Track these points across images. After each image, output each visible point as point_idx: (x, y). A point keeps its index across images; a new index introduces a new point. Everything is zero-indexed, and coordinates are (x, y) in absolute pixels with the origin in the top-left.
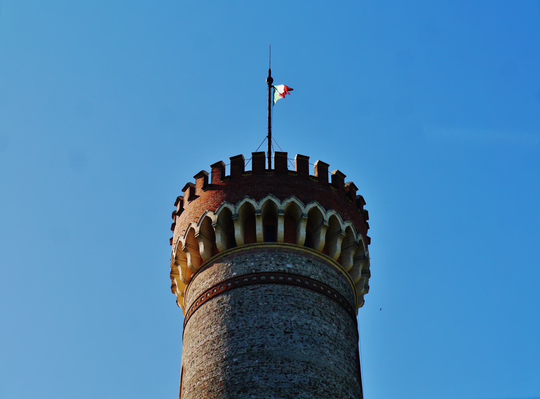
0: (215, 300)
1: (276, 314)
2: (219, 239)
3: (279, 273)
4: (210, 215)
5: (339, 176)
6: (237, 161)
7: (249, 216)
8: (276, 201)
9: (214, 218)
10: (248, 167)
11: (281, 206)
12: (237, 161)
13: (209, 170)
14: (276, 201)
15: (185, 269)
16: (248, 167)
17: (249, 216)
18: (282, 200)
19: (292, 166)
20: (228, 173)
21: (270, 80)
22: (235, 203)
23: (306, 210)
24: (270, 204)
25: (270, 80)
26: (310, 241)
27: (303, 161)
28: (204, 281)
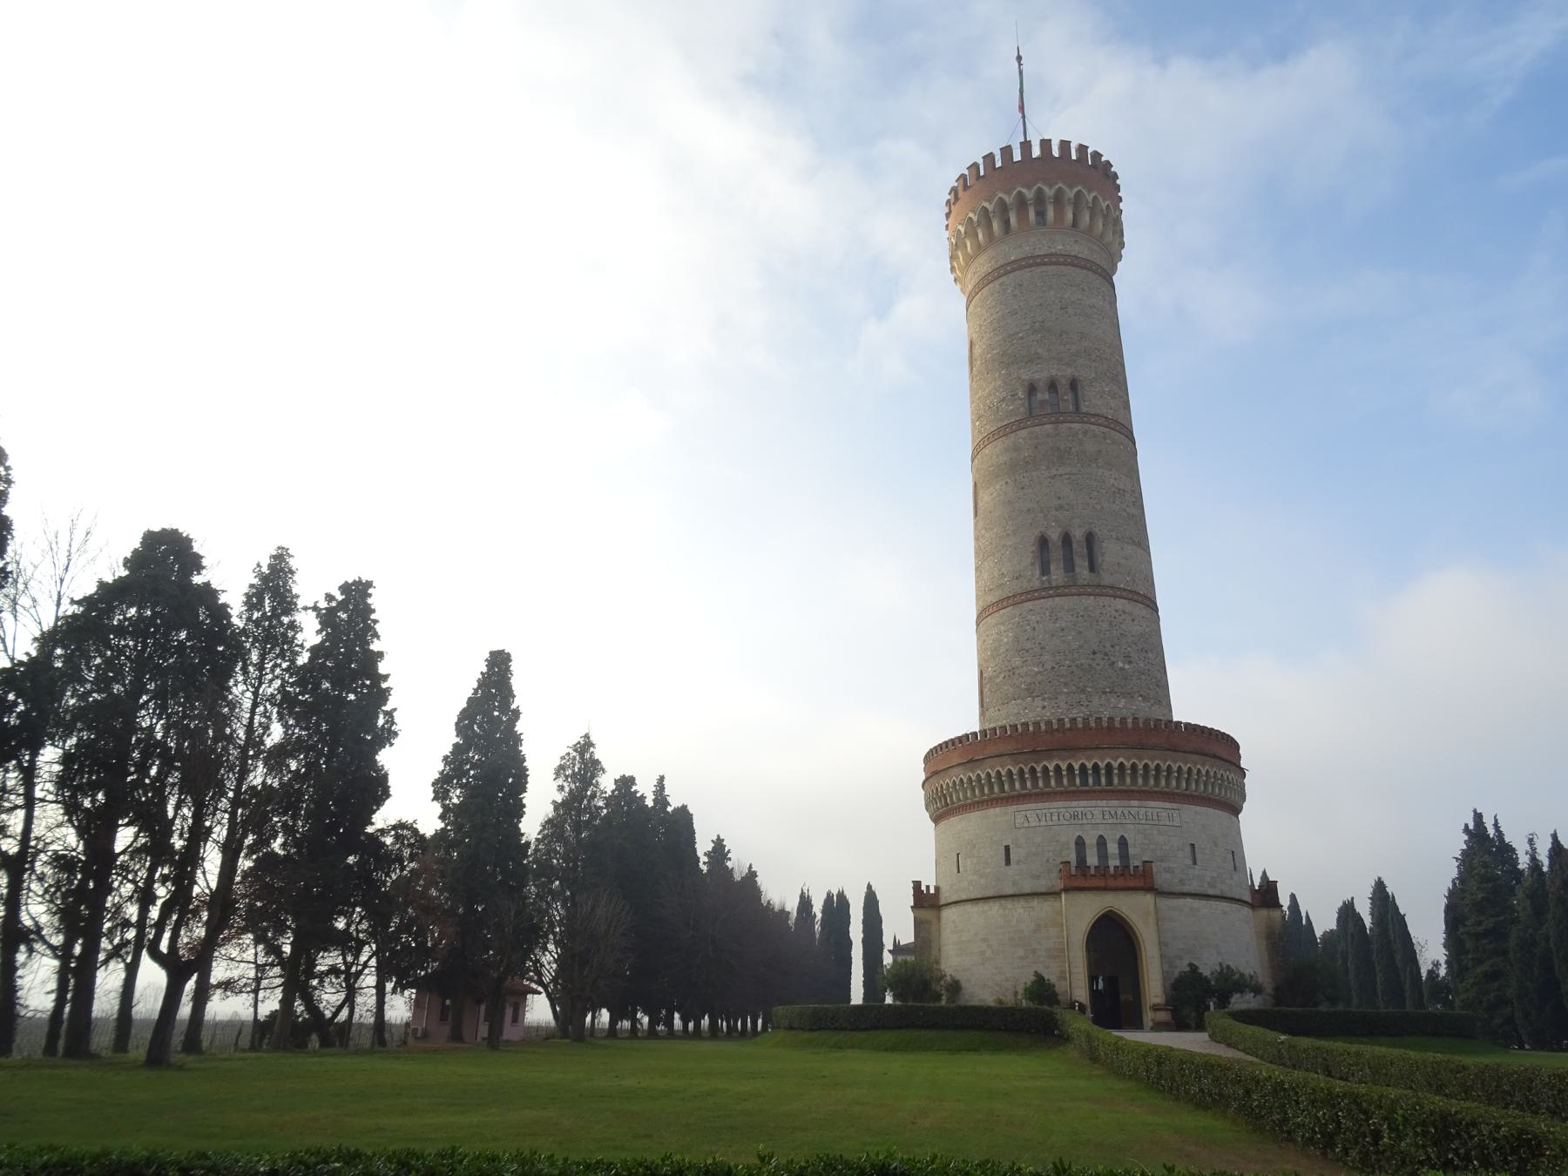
0: (997, 283)
1: (1052, 293)
2: (996, 226)
3: (1052, 254)
4: (986, 204)
5: (1097, 155)
6: (1006, 151)
7: (1022, 203)
8: (1046, 188)
9: (990, 207)
10: (1017, 157)
11: (1049, 192)
12: (1006, 151)
13: (981, 162)
14: (1046, 188)
15: (965, 254)
16: (1017, 157)
17: (1022, 203)
18: (1051, 186)
19: (1056, 153)
20: (998, 164)
21: (1019, 58)
22: (1008, 193)
23: (1070, 194)
24: (1040, 191)
25: (1019, 58)
26: (1075, 224)
27: (1065, 145)
28: (983, 265)
